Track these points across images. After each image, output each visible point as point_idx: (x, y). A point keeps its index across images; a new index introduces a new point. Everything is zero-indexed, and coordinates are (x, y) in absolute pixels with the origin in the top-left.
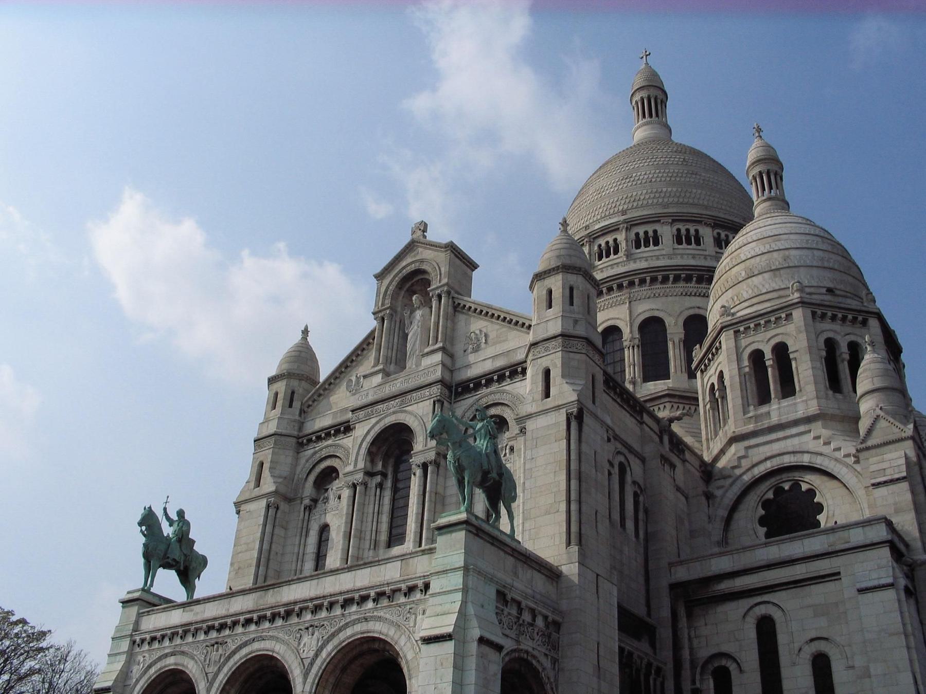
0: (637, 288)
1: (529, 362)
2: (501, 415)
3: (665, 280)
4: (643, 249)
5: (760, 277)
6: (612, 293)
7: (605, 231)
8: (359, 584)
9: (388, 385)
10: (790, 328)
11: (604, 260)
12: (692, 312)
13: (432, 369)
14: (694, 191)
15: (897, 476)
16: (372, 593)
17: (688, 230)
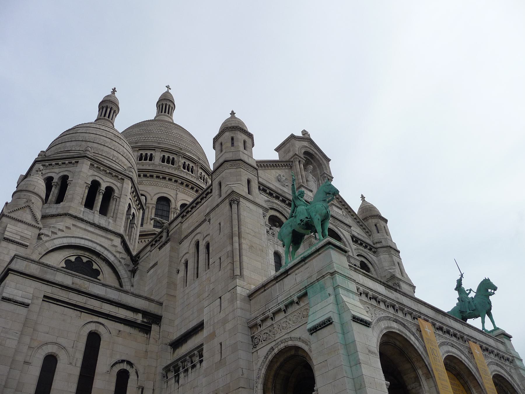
1: (379, 250)
2: (368, 265)
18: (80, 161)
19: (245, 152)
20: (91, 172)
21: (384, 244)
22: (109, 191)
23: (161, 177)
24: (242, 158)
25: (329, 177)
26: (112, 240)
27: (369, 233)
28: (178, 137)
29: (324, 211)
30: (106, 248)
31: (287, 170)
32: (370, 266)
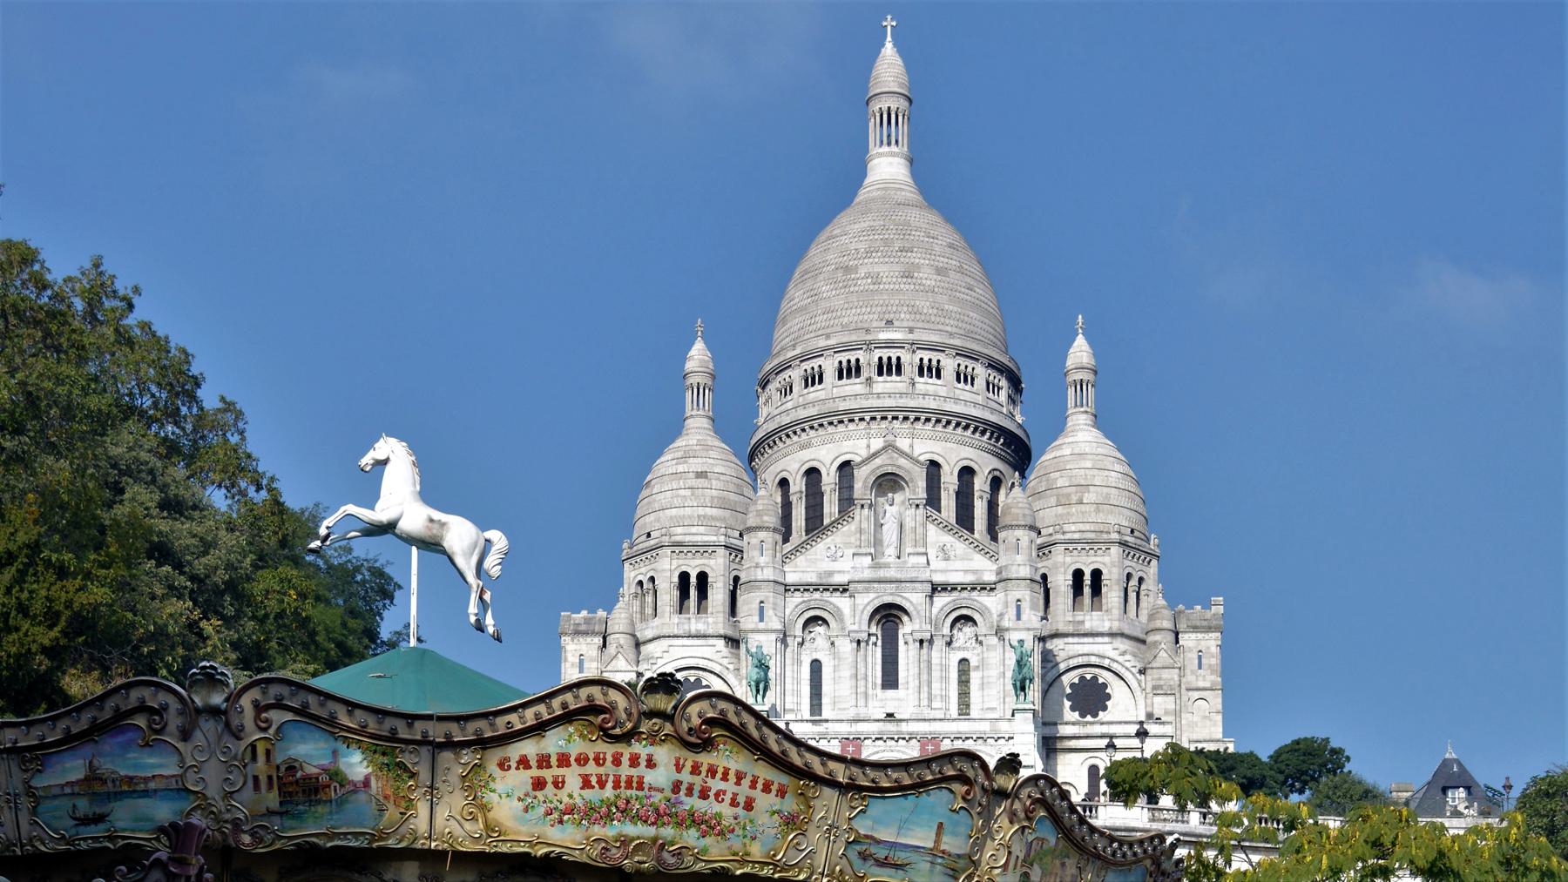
0: (919, 425)
1: (998, 586)
3: (949, 422)
4: (925, 379)
5: (1088, 506)
6: (895, 421)
7: (890, 345)
8: (961, 729)
9: (882, 570)
10: (1107, 559)
11: (885, 377)
12: (966, 463)
13: (922, 569)
14: (971, 314)
15: (1169, 692)
16: (975, 738)
17: (966, 367)
18: (660, 552)
19: (762, 560)
20: (675, 563)
21: (1004, 575)
22: (703, 577)
23: (835, 422)
24: (753, 578)
25: (917, 502)
26: (714, 646)
27: (993, 557)
28: (866, 287)
29: (755, 677)
30: (709, 659)
31: (844, 529)
32: (976, 617)
